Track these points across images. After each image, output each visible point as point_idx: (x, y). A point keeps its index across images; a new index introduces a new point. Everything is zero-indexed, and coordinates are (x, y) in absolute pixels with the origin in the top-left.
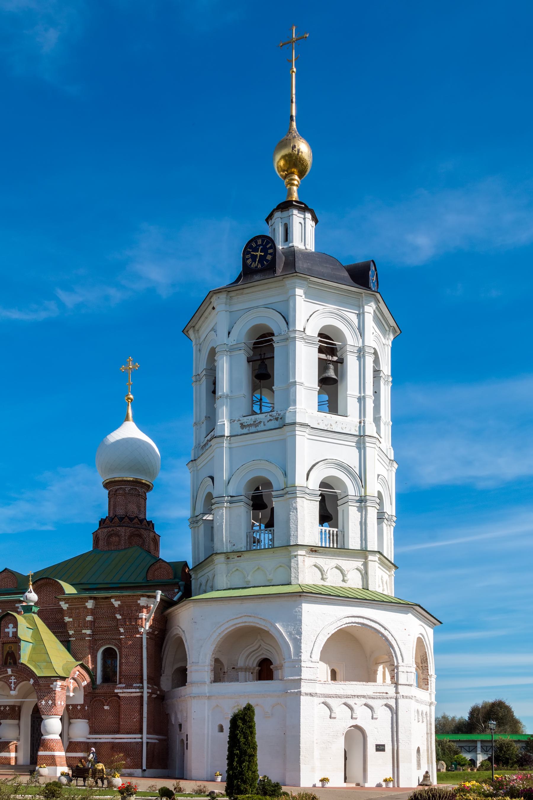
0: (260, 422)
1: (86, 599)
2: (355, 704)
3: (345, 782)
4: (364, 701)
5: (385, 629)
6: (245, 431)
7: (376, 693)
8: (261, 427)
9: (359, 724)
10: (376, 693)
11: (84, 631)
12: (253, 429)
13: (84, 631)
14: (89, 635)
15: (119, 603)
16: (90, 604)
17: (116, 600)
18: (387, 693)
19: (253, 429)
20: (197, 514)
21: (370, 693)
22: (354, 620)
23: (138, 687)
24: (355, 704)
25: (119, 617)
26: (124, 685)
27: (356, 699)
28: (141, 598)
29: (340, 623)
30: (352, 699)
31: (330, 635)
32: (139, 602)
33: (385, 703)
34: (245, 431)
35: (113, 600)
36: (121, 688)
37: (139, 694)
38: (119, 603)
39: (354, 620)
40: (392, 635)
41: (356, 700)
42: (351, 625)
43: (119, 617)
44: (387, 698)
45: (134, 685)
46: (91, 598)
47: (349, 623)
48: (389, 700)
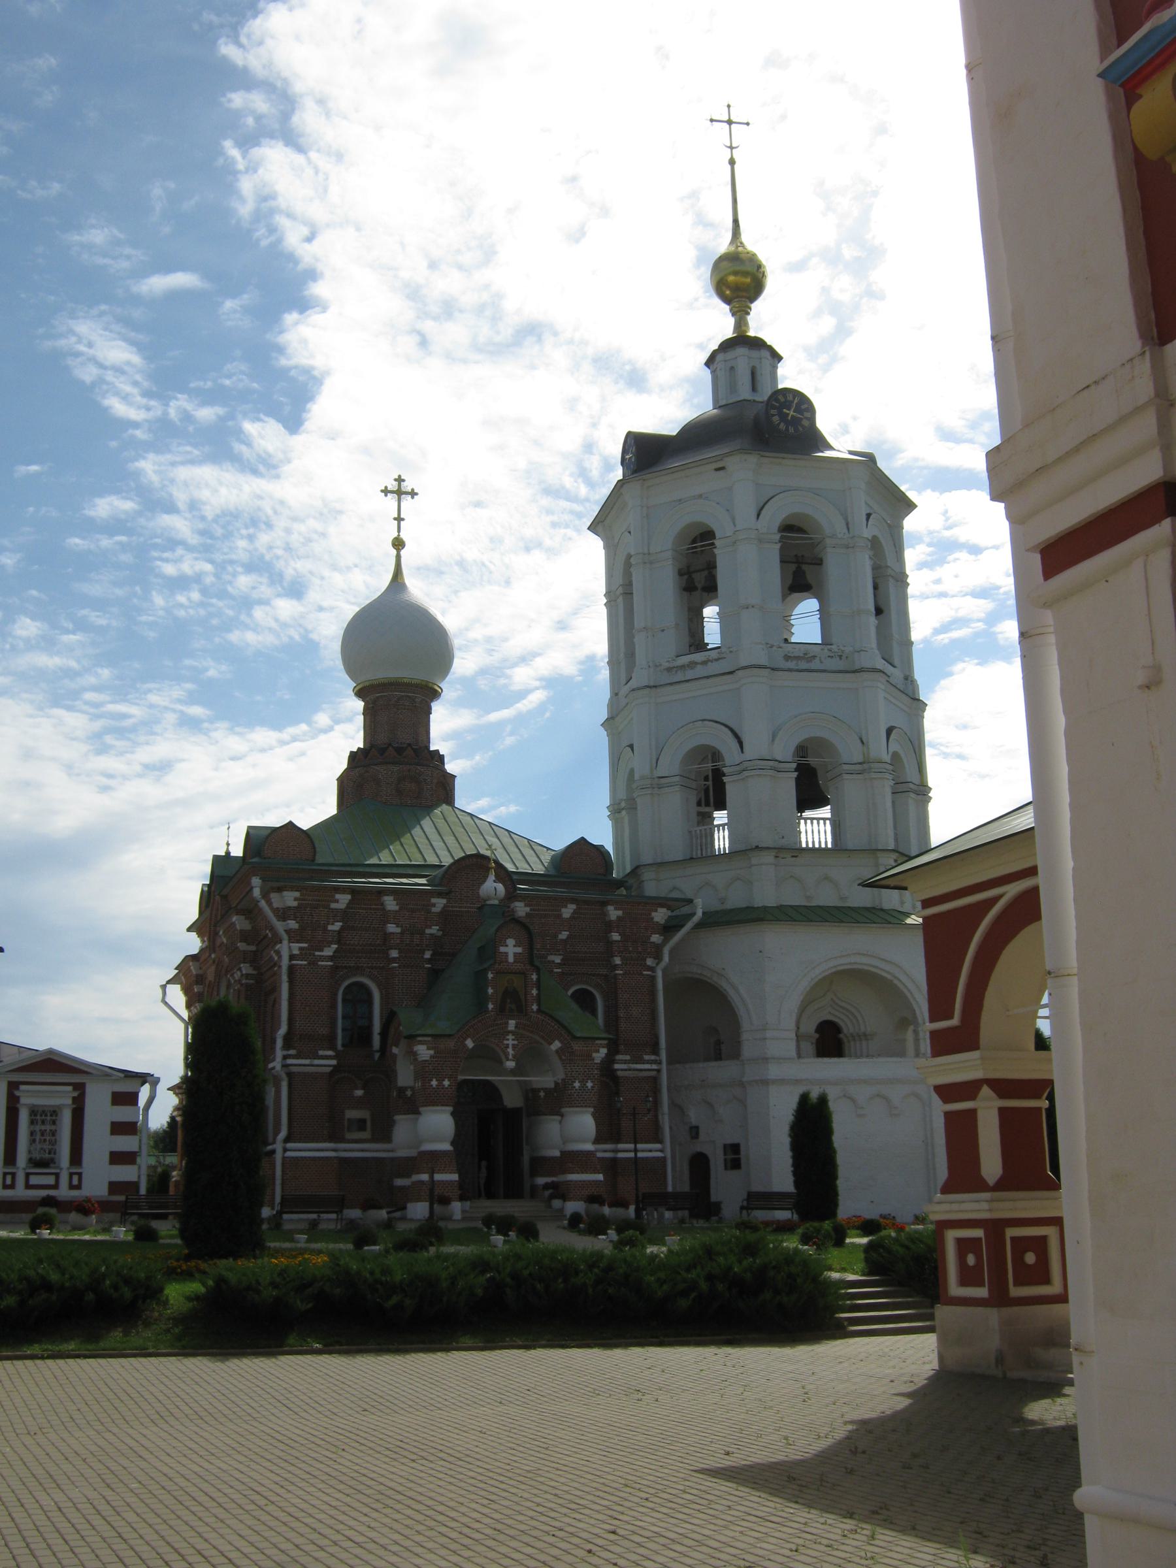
0: (814, 657)
1: (565, 901)
6: (791, 664)
8: (815, 665)
11: (551, 958)
12: (803, 665)
13: (551, 958)
14: (559, 965)
15: (620, 913)
16: (567, 911)
17: (616, 909)
19: (803, 665)
20: (660, 772)
23: (654, 1062)
25: (616, 937)
26: (628, 1057)
28: (660, 910)
32: (654, 914)
34: (791, 664)
35: (610, 908)
36: (625, 1062)
37: (653, 1074)
38: (620, 913)
43: (616, 937)
45: (646, 1057)
46: (573, 900)
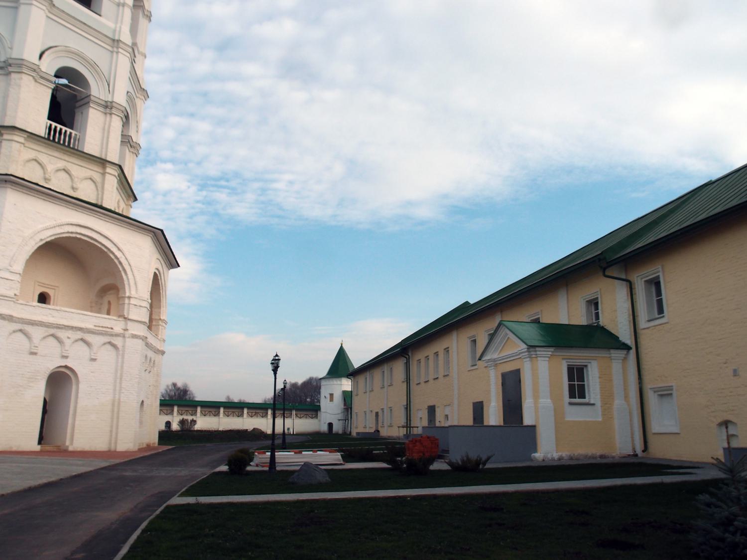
2: (69, 338)
3: (40, 443)
4: (79, 335)
5: (119, 249)
7: (99, 326)
9: (69, 365)
10: (99, 326)
18: (112, 328)
21: (90, 326)
22: (79, 230)
24: (69, 338)
27: (70, 332)
29: (58, 230)
30: (63, 331)
31: (44, 242)
33: (109, 341)
39: (79, 230)
40: (126, 259)
41: (69, 333)
42: (74, 235)
44: (112, 335)
47: (72, 233)
48: (115, 338)
